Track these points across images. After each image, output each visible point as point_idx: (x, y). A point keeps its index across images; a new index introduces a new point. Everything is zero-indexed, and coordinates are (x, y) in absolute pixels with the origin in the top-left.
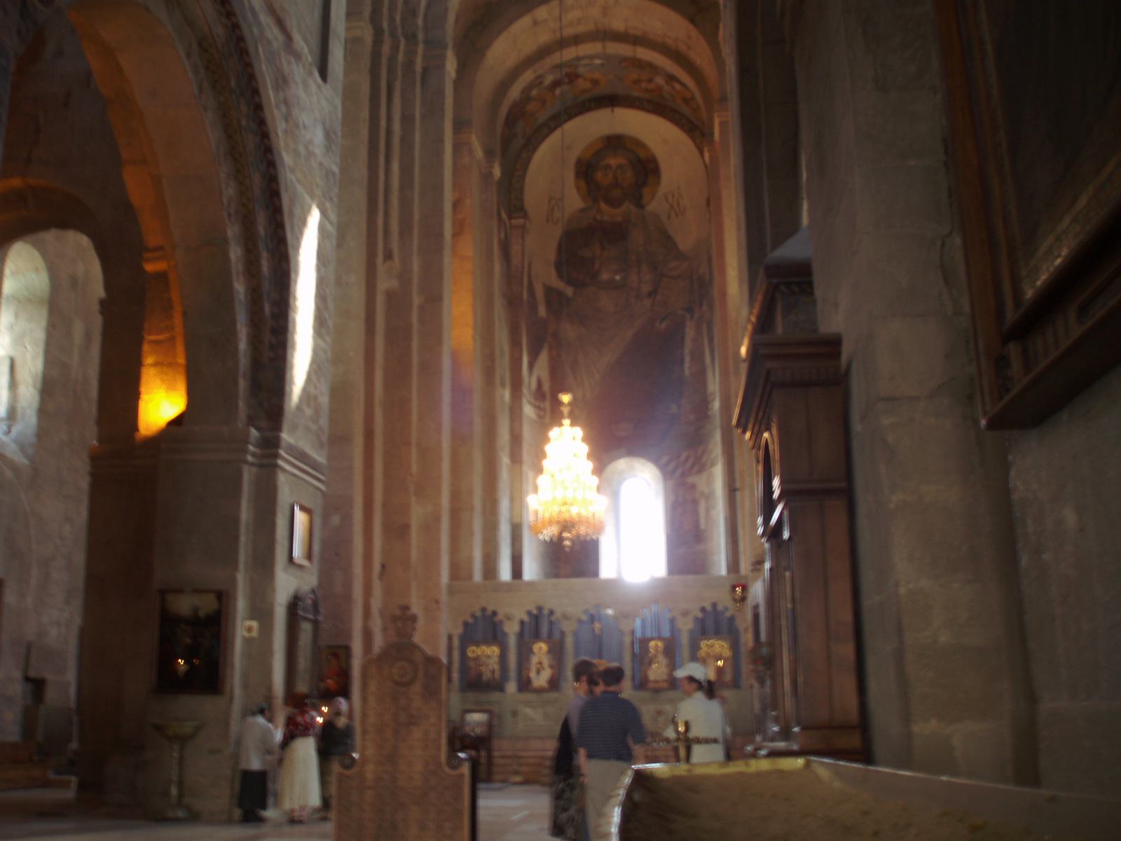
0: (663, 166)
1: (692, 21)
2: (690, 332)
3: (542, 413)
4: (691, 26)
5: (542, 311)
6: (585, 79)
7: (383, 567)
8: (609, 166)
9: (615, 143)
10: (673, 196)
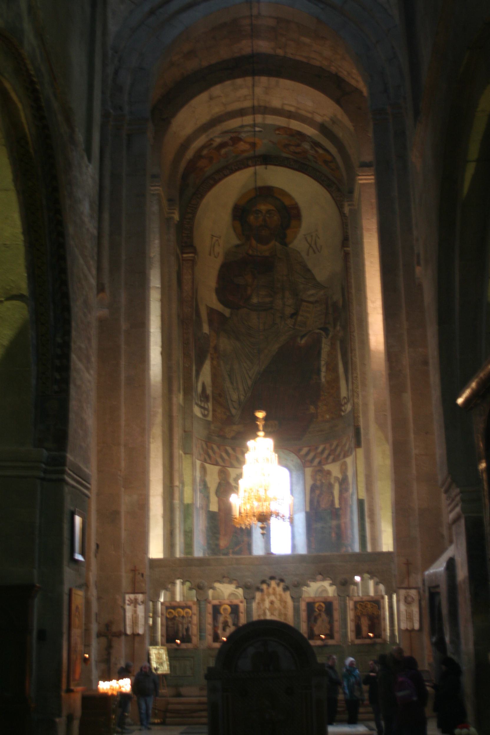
0: (304, 213)
1: (338, 102)
2: (325, 348)
3: (206, 412)
4: (337, 107)
5: (206, 329)
6: (245, 142)
7: (98, 546)
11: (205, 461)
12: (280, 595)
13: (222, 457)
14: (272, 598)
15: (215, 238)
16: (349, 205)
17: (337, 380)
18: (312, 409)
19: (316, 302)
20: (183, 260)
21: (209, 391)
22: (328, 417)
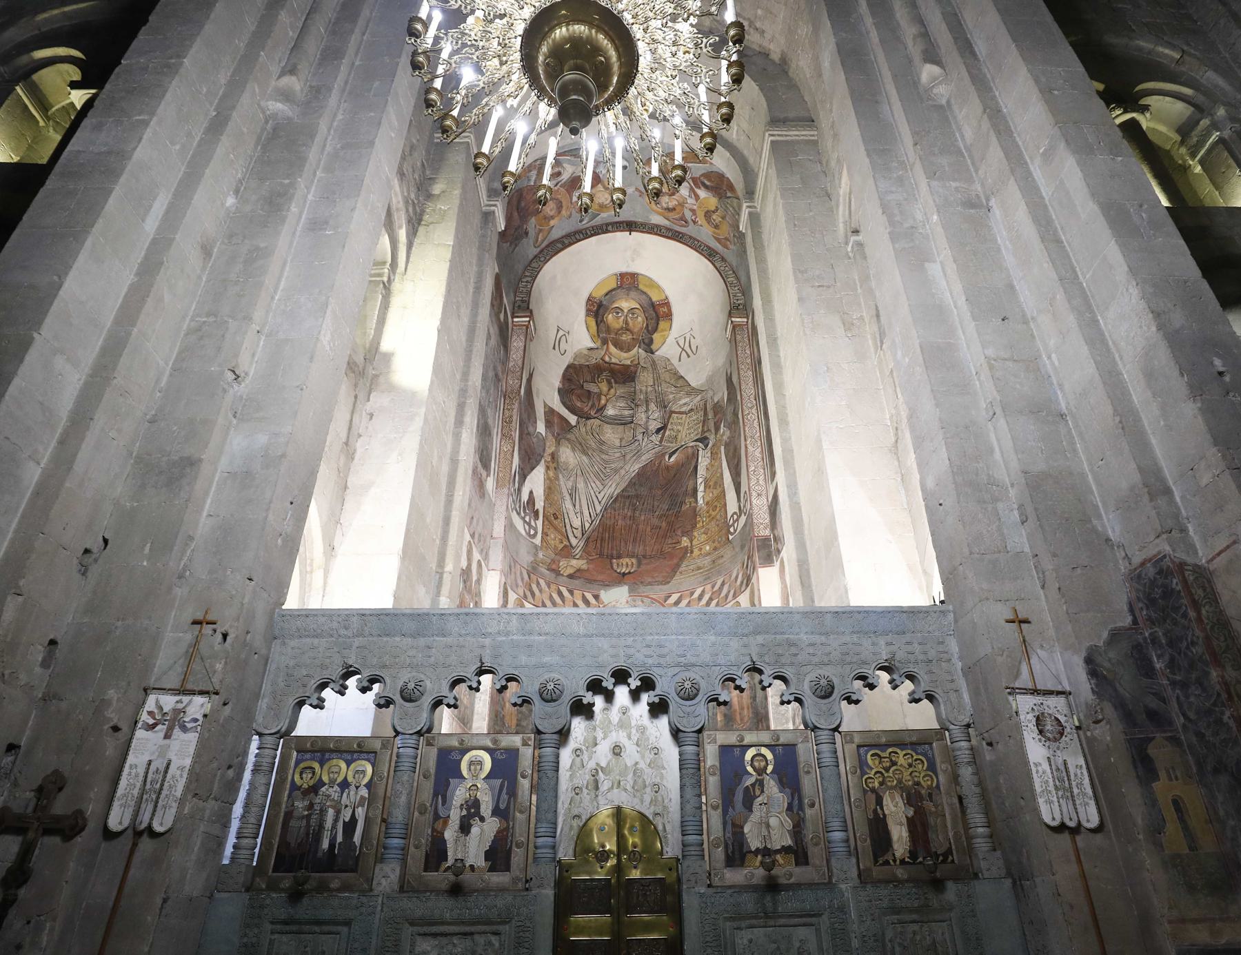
2: (704, 461)
5: (541, 428)
8: (622, 310)
9: (628, 282)
10: (685, 338)
11: (525, 597)
12: (642, 730)
13: (551, 597)
14: (620, 737)
15: (561, 333)
16: (748, 207)
21: (539, 505)
22: (708, 548)
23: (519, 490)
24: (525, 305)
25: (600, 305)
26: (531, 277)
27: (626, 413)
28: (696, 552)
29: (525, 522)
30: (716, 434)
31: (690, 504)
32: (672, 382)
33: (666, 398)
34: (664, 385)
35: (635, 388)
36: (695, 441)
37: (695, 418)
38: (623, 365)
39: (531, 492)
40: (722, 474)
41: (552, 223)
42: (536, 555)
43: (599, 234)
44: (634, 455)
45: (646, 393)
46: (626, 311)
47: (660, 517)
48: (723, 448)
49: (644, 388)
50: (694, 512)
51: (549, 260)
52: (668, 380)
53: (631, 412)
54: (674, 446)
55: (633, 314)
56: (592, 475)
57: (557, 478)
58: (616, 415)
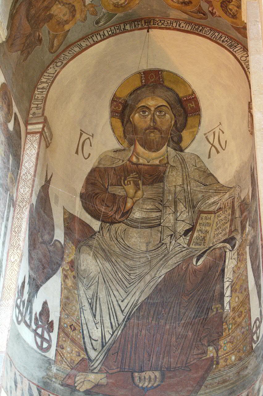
2: (230, 264)
3: (45, 345)
5: (59, 235)
8: (149, 109)
15: (84, 136)
17: (246, 301)
18: (211, 352)
19: (220, 209)
20: (27, 133)
21: (55, 316)
22: (233, 358)
23: (30, 301)
24: (40, 111)
25: (125, 105)
26: (46, 82)
27: (154, 215)
28: (222, 363)
29: (36, 334)
30: (242, 233)
31: (217, 310)
32: (201, 180)
33: (195, 198)
34: (193, 184)
35: (163, 188)
36: (224, 241)
37: (223, 217)
38: (150, 165)
39: (45, 303)
40: (247, 277)
41: (67, 27)
42: (49, 369)
43: (116, 34)
44: (161, 260)
45: (175, 193)
46: (153, 109)
47: (185, 326)
48: (248, 247)
49: (172, 189)
50: (221, 319)
51: (66, 64)
52: (197, 178)
53: (158, 214)
54: (202, 248)
55: (160, 112)
56: (115, 283)
57: (76, 287)
58: (143, 218)
